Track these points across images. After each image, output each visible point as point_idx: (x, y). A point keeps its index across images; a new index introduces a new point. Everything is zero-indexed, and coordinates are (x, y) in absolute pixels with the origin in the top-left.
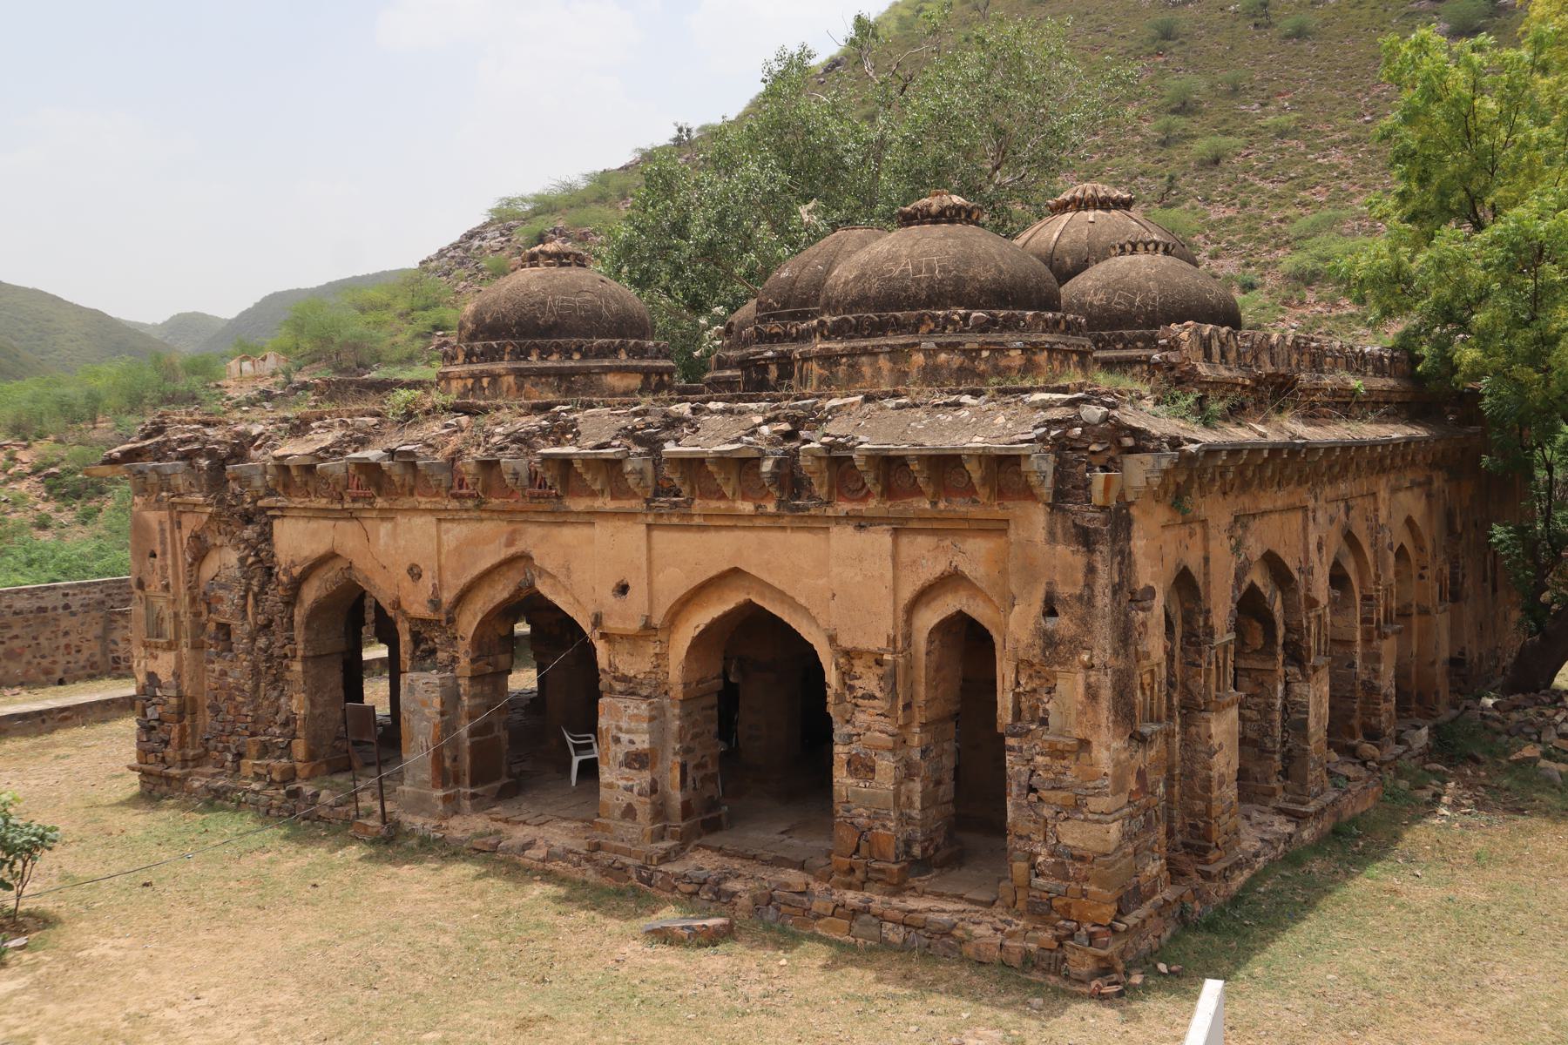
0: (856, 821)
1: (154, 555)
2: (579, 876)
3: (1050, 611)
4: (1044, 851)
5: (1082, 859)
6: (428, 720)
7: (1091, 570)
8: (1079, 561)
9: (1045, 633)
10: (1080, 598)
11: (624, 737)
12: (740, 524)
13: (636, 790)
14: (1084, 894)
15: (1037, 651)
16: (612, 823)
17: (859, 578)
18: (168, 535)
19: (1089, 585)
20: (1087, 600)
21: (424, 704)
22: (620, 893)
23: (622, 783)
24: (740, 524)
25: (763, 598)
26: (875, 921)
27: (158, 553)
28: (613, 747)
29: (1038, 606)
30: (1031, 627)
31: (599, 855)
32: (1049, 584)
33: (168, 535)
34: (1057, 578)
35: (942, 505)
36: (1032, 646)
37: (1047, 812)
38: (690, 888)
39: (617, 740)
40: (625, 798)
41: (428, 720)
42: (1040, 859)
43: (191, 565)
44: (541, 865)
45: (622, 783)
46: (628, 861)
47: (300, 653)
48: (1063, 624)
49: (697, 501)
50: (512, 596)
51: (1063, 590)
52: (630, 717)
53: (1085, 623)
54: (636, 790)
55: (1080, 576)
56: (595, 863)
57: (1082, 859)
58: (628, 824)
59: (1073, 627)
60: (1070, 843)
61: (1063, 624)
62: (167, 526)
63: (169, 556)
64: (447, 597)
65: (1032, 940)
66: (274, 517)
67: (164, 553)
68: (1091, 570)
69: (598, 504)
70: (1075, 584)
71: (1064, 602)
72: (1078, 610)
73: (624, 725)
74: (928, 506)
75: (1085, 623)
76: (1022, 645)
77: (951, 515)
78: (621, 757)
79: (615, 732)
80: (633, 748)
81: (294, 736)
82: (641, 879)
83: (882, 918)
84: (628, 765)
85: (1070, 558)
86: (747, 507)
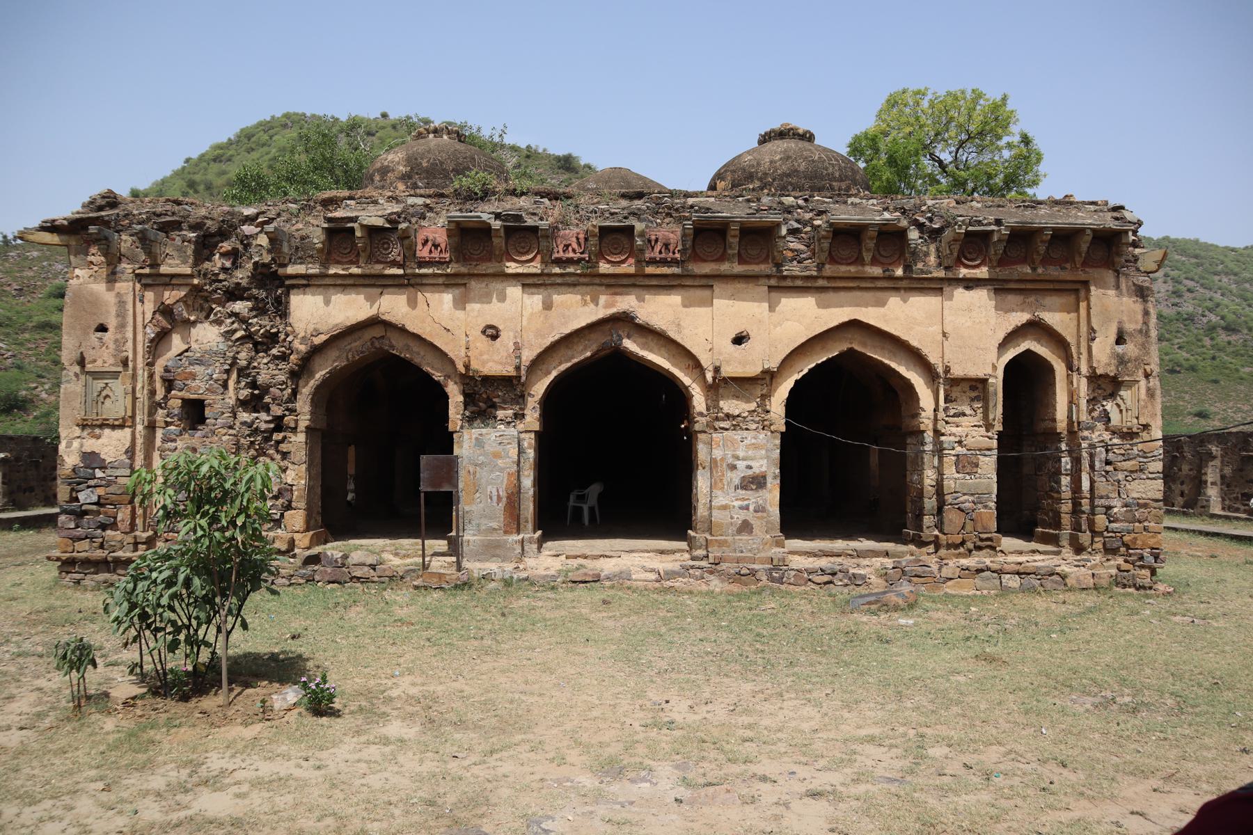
0: (962, 506)
1: (102, 328)
2: (704, 588)
3: (1120, 340)
4: (1119, 504)
5: (1145, 506)
6: (502, 470)
7: (1146, 313)
8: (1139, 308)
9: (1118, 355)
10: (1140, 331)
11: (741, 465)
12: (864, 285)
13: (751, 508)
14: (1145, 529)
15: (1113, 368)
16: (729, 538)
17: (969, 324)
18: (130, 307)
19: (1145, 323)
20: (1145, 333)
21: (497, 455)
22: (759, 592)
23: (737, 504)
24: (864, 285)
25: (865, 345)
26: (995, 575)
27: (112, 323)
28: (729, 474)
29: (1113, 337)
30: (1108, 351)
31: (724, 566)
32: (1120, 322)
33: (130, 307)
34: (1125, 319)
35: (1040, 270)
36: (1109, 365)
37: (1121, 476)
38: (826, 578)
39: (733, 467)
40: (740, 517)
41: (502, 470)
42: (1115, 510)
43: (152, 341)
44: (657, 585)
45: (737, 504)
46: (756, 567)
47: (303, 424)
48: (1130, 349)
49: (827, 266)
50: (592, 356)
51: (1129, 327)
52: (748, 447)
53: (1144, 347)
54: (751, 508)
55: (1140, 317)
56: (720, 574)
57: (1145, 506)
58: (745, 537)
59: (1137, 351)
60: (1135, 495)
61: (1130, 349)
62: (130, 299)
63: (130, 329)
64: (528, 355)
65: (1109, 567)
66: (293, 286)
67: (122, 326)
68: (1146, 313)
69: (725, 267)
70: (1137, 323)
71: (1131, 335)
72: (1140, 339)
73: (741, 454)
74: (1029, 271)
75: (1144, 347)
76: (1102, 364)
77: (1047, 278)
78: (737, 481)
79: (730, 461)
80: (750, 472)
81: (289, 507)
82: (772, 579)
83: (1000, 572)
84: (744, 487)
85: (1132, 306)
86: (877, 271)
